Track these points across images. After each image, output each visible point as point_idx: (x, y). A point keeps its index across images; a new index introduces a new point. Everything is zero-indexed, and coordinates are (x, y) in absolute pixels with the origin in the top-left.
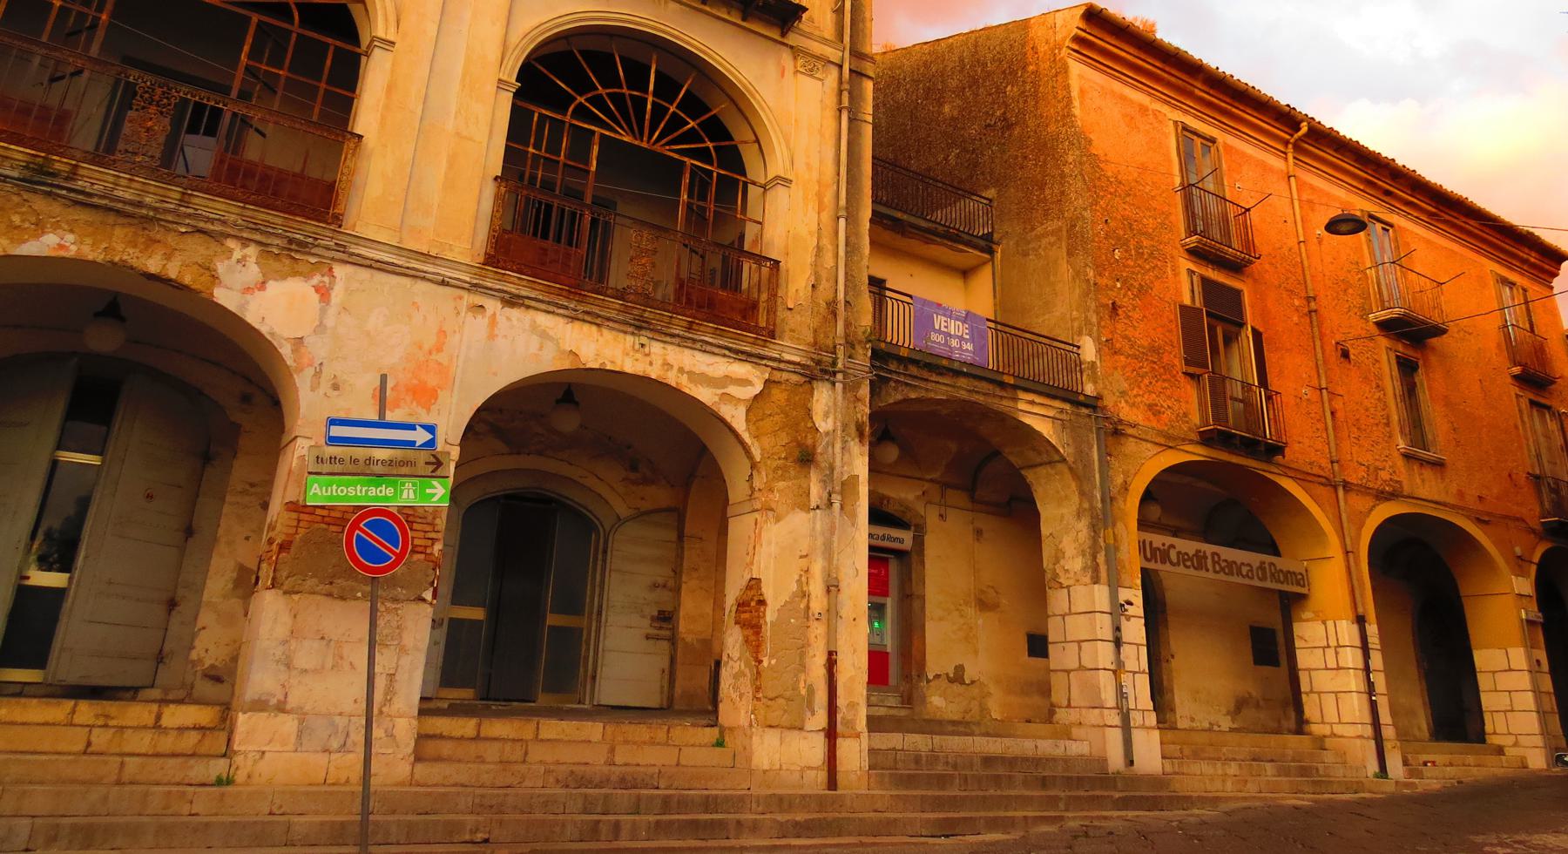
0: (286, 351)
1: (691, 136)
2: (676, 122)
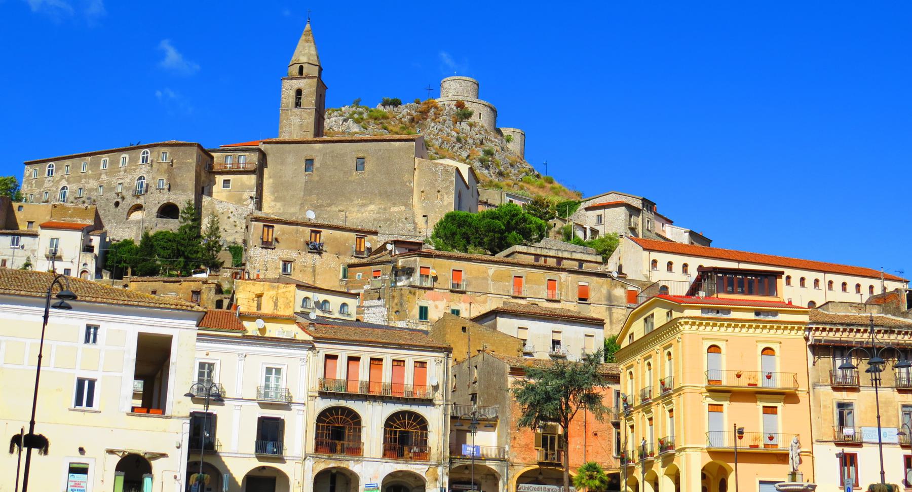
0: (358, 474)
1: (415, 426)
2: (412, 424)
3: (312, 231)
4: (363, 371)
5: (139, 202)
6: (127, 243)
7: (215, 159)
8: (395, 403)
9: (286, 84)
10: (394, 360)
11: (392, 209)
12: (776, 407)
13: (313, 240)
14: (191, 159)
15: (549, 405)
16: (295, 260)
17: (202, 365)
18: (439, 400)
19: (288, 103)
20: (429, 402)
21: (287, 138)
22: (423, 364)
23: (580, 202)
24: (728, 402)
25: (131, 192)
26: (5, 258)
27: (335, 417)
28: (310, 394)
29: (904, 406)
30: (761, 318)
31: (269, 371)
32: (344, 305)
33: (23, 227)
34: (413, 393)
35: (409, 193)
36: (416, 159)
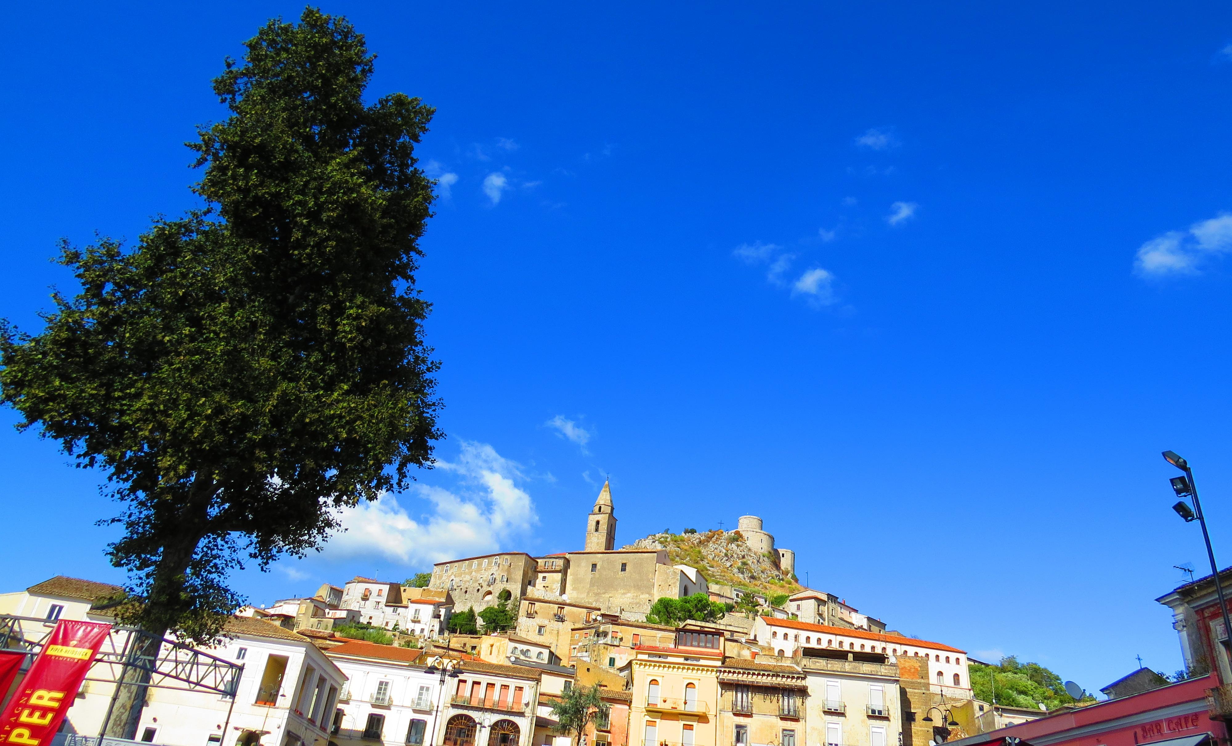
3: (559, 607)
4: (481, 692)
5: (490, 589)
6: (462, 613)
10: (502, 685)
14: (520, 563)
17: (381, 683)
21: (589, 551)
22: (521, 689)
23: (789, 596)
25: (486, 583)
26: (388, 620)
29: (784, 730)
30: (689, 662)
31: (422, 688)
32: (540, 653)
33: (405, 603)
34: (512, 708)
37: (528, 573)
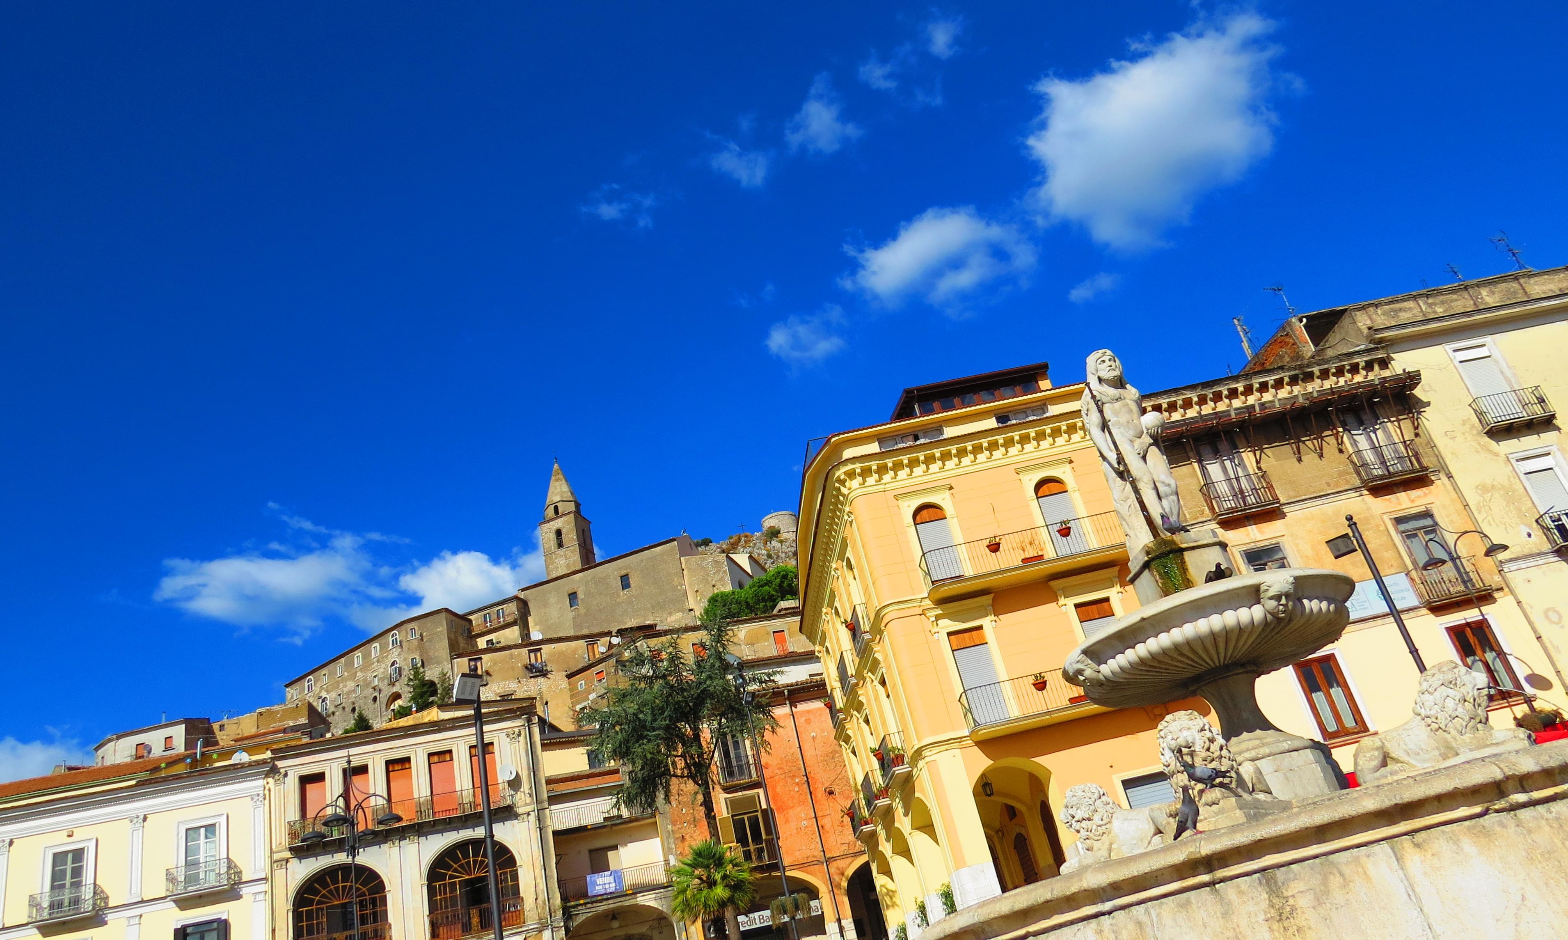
3: (530, 651)
5: (395, 689)
7: (474, 622)
8: (441, 832)
9: (545, 527)
10: (430, 755)
11: (669, 620)
12: (1107, 600)
13: (533, 661)
15: (643, 744)
16: (515, 691)
18: (526, 805)
19: (550, 547)
20: (507, 814)
24: (993, 617)
25: (386, 682)
27: (332, 887)
28: (276, 857)
29: (1399, 521)
35: (683, 596)
36: (682, 559)
37: (457, 642)
